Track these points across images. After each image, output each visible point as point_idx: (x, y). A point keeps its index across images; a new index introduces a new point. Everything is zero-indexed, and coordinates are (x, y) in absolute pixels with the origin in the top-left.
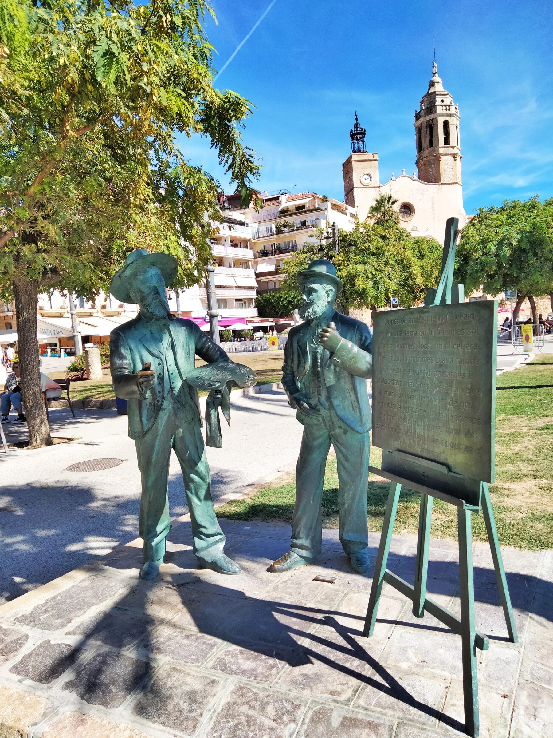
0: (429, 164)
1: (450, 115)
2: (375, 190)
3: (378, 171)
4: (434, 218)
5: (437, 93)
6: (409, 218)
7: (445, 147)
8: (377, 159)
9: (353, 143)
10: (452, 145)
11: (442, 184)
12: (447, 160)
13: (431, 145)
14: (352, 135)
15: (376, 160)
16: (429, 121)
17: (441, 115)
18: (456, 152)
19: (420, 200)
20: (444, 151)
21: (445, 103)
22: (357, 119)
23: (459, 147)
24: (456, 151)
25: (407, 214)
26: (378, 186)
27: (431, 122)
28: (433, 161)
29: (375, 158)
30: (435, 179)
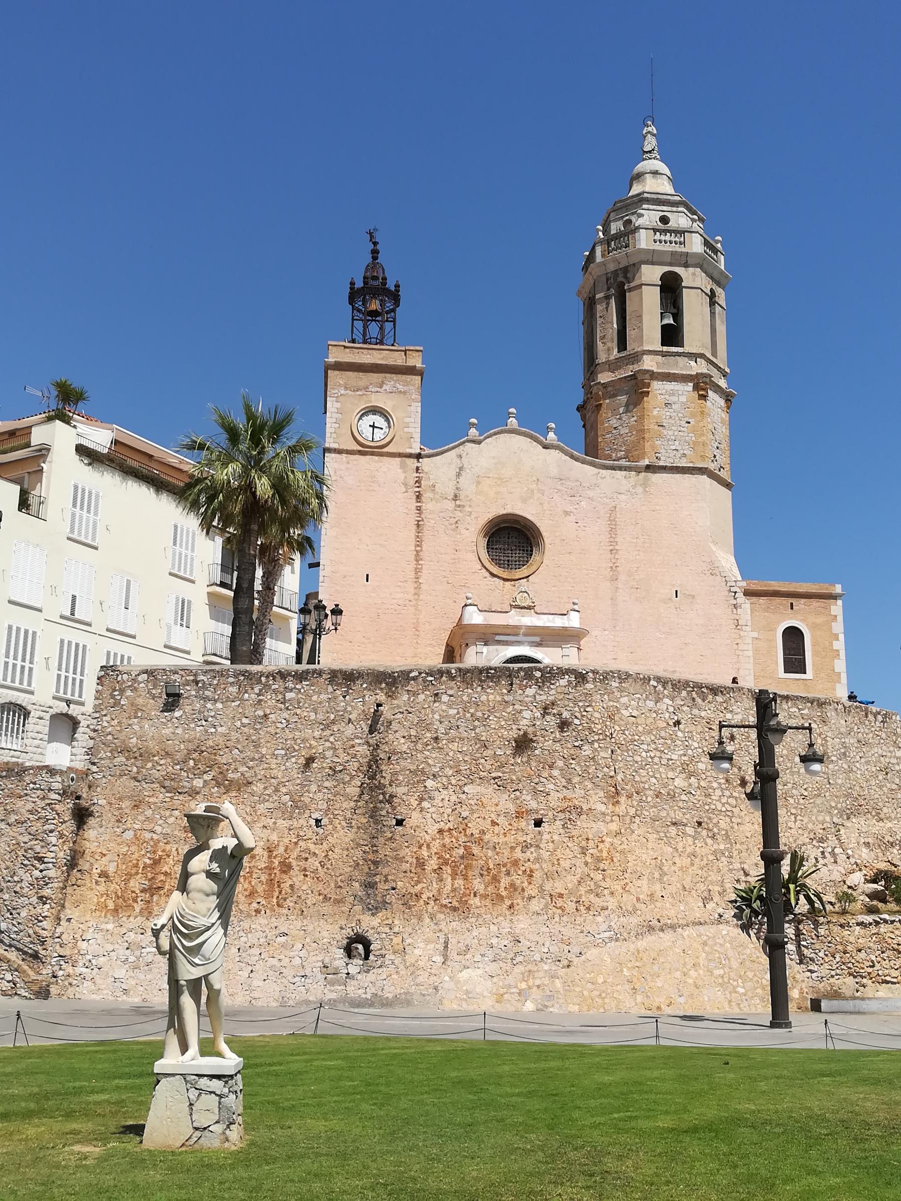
1: (686, 260)
2: (403, 466)
3: (417, 407)
4: (614, 579)
5: (646, 195)
6: (524, 571)
7: (664, 354)
8: (419, 365)
9: (353, 320)
11: (649, 468)
13: (622, 344)
14: (354, 295)
15: (410, 371)
16: (615, 273)
17: (653, 258)
18: (705, 371)
19: (567, 513)
21: (672, 224)
22: (375, 253)
23: (722, 360)
24: (700, 367)
25: (517, 555)
26: (418, 451)
29: (411, 362)
30: (627, 451)
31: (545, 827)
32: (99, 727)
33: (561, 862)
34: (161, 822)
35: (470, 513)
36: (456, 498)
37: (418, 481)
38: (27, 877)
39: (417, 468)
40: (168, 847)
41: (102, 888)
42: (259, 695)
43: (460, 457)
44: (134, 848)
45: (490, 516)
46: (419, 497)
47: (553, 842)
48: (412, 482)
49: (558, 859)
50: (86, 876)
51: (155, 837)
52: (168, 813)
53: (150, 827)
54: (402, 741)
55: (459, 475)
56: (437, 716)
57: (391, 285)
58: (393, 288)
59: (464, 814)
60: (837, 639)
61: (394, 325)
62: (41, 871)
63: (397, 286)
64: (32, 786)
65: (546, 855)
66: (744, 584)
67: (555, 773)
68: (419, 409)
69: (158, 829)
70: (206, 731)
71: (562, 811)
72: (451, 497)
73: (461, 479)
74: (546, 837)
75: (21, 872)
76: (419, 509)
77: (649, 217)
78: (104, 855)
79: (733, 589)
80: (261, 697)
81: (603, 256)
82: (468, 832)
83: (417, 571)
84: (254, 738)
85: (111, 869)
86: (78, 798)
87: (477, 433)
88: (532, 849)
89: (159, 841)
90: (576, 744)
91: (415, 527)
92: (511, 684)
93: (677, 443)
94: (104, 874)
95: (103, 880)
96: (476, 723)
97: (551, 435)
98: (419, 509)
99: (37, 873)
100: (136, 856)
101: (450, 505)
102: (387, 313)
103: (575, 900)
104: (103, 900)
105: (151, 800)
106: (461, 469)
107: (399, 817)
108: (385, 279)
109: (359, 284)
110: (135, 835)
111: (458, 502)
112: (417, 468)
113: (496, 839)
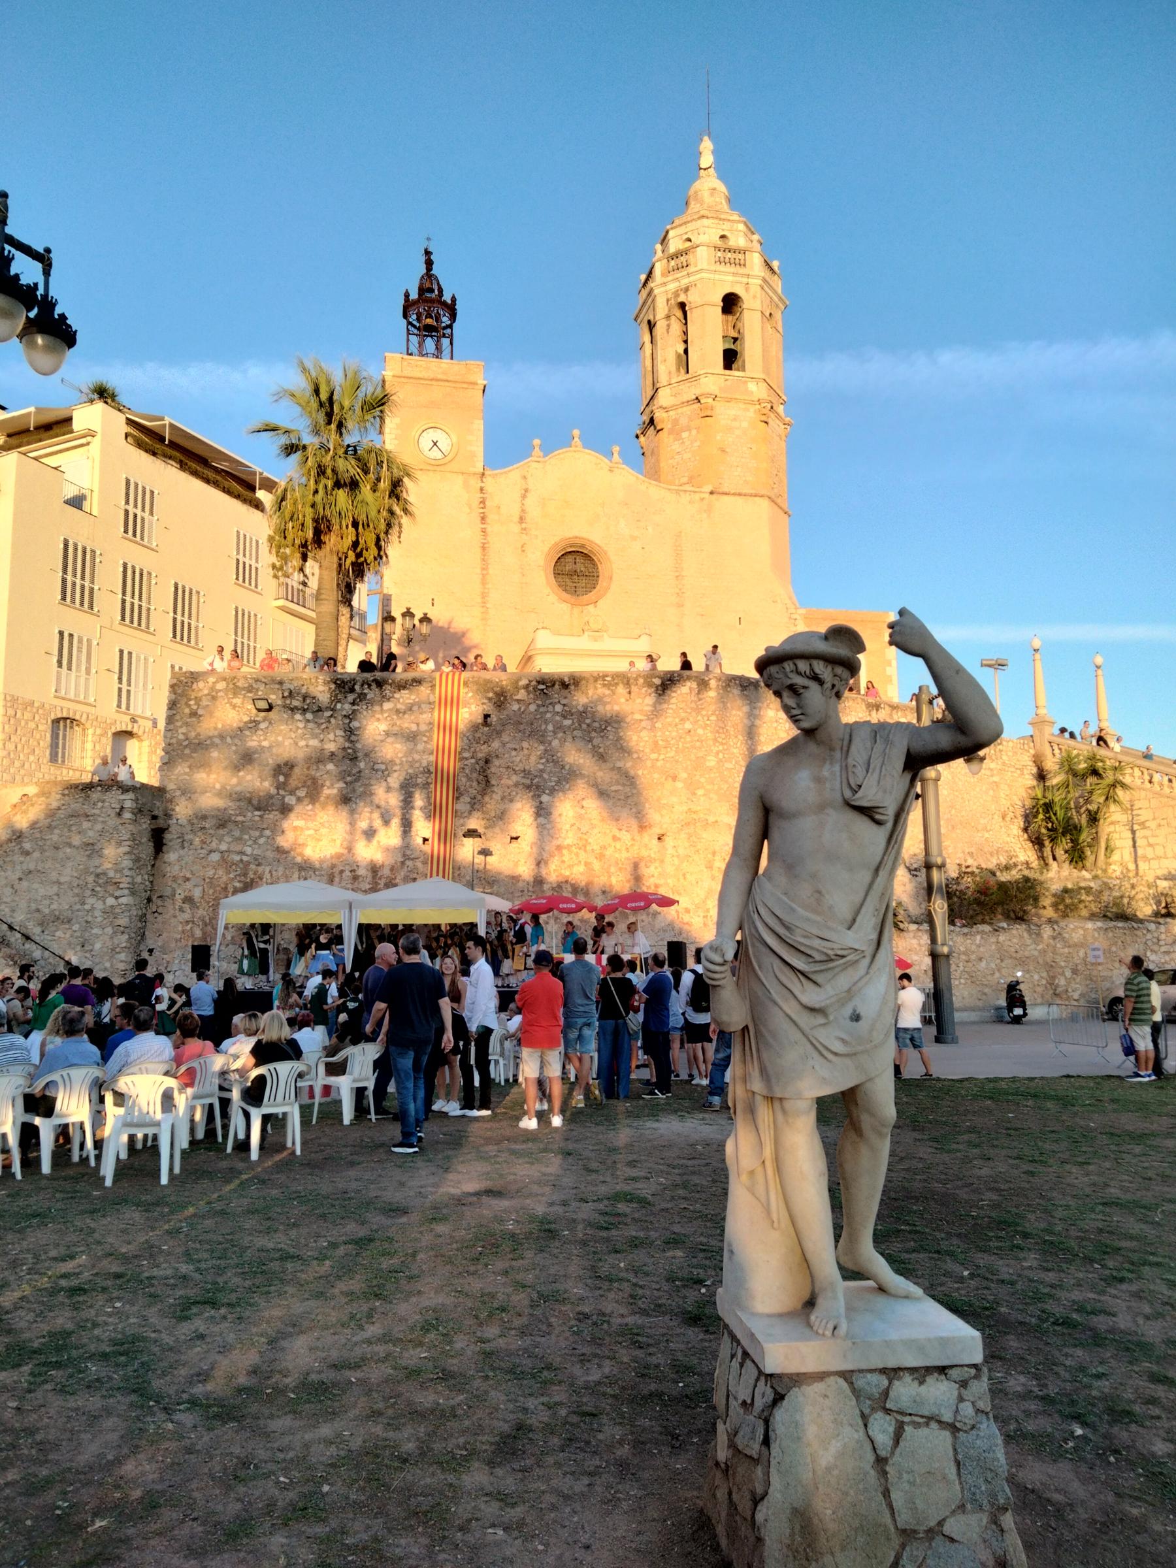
0: (671, 432)
3: (479, 425)
4: (680, 605)
6: (592, 595)
9: (409, 334)
10: (748, 373)
11: (712, 493)
12: (735, 419)
14: (408, 306)
16: (676, 294)
19: (634, 538)
20: (720, 388)
22: (429, 264)
27: (682, 298)
28: (683, 421)
30: (691, 478)
31: (669, 841)
32: (174, 741)
33: (688, 876)
34: (250, 843)
35: (536, 536)
36: (522, 520)
37: (483, 502)
38: (99, 905)
39: (482, 489)
40: (260, 869)
41: (186, 916)
42: (353, 704)
43: (525, 477)
44: (220, 872)
45: (557, 539)
46: (483, 519)
47: (678, 856)
48: (475, 503)
49: (684, 875)
50: (168, 903)
51: (245, 858)
52: (257, 833)
53: (238, 848)
54: (514, 753)
55: (524, 497)
56: (550, 727)
57: (447, 298)
58: (449, 302)
59: (584, 829)
60: (890, 665)
61: (451, 344)
62: (117, 898)
63: (454, 299)
64: (100, 804)
65: (670, 869)
66: (802, 611)
67: (679, 785)
68: (482, 427)
69: (248, 850)
70: (296, 744)
71: (688, 824)
72: (516, 519)
73: (528, 501)
74: (670, 851)
75: (91, 901)
76: (484, 531)
77: (707, 233)
78: (188, 879)
79: (794, 616)
80: (356, 707)
81: (663, 275)
82: (588, 848)
83: (484, 595)
84: (350, 751)
85: (197, 893)
86: (154, 817)
87: (541, 454)
88: (657, 864)
89: (249, 863)
90: (701, 754)
91: (479, 550)
92: (630, 693)
93: (739, 469)
94: (189, 900)
95: (186, 906)
96: (594, 734)
97: (616, 456)
98: (484, 531)
99: (111, 901)
100: (225, 878)
101: (516, 528)
102: (445, 328)
103: (702, 914)
104: (188, 928)
105: (240, 818)
106: (526, 490)
107: (514, 835)
108: (441, 290)
109: (414, 295)
110: (222, 857)
111: (524, 525)
112: (482, 489)
113: (617, 855)
